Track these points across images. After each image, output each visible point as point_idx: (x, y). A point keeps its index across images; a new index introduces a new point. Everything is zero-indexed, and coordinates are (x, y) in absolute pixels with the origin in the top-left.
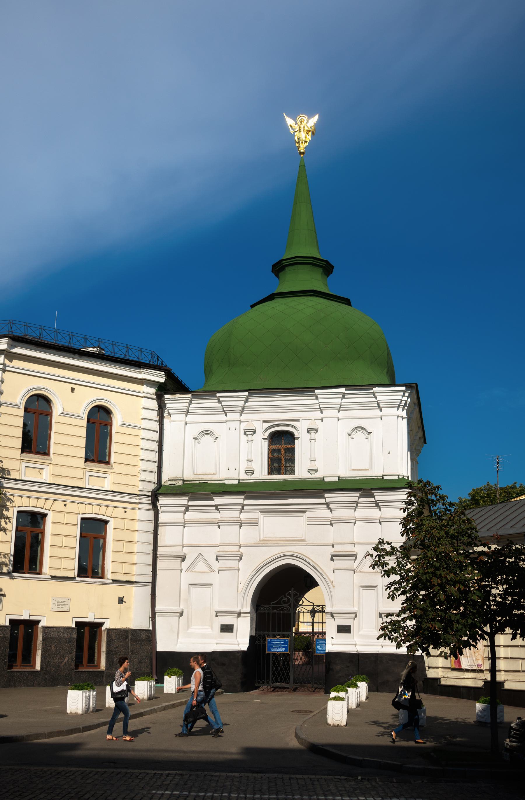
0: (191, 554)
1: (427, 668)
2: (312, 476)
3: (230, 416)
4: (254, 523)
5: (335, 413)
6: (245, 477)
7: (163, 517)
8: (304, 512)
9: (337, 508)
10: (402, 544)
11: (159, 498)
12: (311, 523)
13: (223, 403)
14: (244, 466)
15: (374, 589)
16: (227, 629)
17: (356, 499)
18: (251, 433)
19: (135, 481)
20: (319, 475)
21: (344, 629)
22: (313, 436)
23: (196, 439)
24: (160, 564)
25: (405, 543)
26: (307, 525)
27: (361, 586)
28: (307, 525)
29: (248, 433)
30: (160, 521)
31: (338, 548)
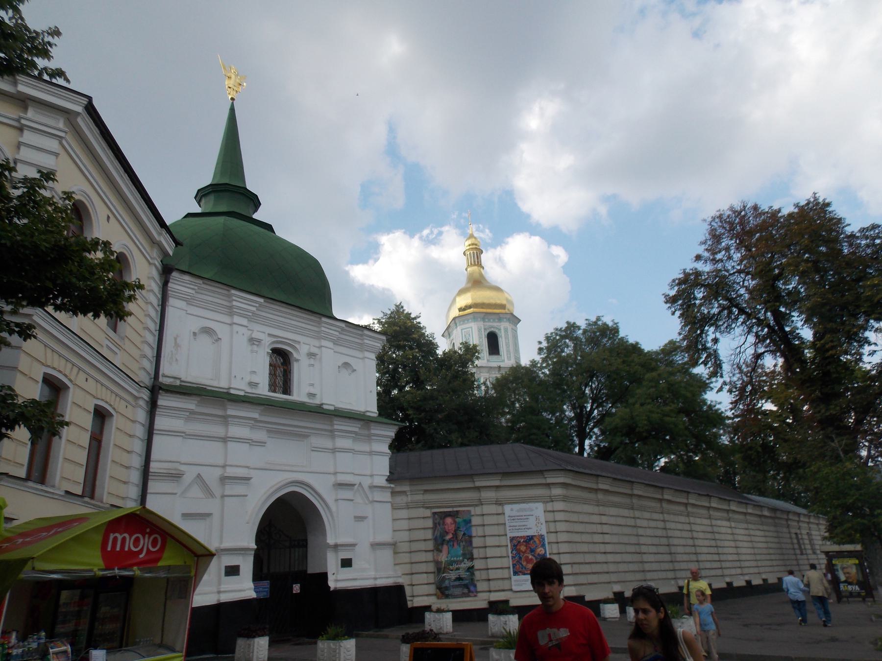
0: (190, 474)
1: (408, 598)
2: (311, 401)
3: (237, 319)
4: (262, 444)
5: (330, 345)
6: (249, 390)
7: (161, 422)
8: (306, 436)
9: (340, 436)
10: (386, 477)
11: (160, 397)
12: (315, 449)
13: (234, 303)
14: (248, 379)
15: (363, 521)
16: (232, 571)
17: (356, 430)
18: (257, 343)
19: (134, 366)
20: (317, 401)
21: (347, 563)
22: (312, 361)
23: (195, 334)
24: (152, 486)
25: (389, 476)
26: (313, 450)
27: (355, 517)
28: (313, 450)
29: (255, 342)
30: (156, 427)
31: (342, 478)
